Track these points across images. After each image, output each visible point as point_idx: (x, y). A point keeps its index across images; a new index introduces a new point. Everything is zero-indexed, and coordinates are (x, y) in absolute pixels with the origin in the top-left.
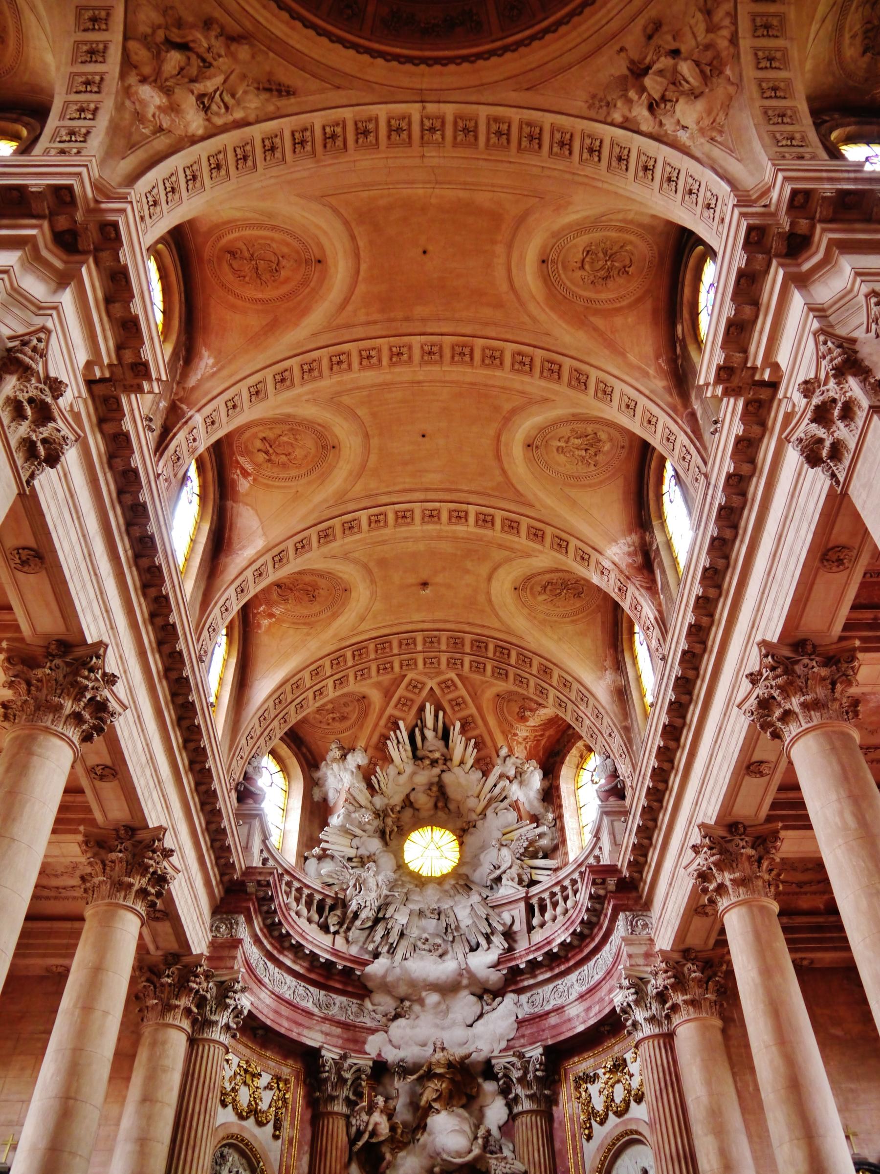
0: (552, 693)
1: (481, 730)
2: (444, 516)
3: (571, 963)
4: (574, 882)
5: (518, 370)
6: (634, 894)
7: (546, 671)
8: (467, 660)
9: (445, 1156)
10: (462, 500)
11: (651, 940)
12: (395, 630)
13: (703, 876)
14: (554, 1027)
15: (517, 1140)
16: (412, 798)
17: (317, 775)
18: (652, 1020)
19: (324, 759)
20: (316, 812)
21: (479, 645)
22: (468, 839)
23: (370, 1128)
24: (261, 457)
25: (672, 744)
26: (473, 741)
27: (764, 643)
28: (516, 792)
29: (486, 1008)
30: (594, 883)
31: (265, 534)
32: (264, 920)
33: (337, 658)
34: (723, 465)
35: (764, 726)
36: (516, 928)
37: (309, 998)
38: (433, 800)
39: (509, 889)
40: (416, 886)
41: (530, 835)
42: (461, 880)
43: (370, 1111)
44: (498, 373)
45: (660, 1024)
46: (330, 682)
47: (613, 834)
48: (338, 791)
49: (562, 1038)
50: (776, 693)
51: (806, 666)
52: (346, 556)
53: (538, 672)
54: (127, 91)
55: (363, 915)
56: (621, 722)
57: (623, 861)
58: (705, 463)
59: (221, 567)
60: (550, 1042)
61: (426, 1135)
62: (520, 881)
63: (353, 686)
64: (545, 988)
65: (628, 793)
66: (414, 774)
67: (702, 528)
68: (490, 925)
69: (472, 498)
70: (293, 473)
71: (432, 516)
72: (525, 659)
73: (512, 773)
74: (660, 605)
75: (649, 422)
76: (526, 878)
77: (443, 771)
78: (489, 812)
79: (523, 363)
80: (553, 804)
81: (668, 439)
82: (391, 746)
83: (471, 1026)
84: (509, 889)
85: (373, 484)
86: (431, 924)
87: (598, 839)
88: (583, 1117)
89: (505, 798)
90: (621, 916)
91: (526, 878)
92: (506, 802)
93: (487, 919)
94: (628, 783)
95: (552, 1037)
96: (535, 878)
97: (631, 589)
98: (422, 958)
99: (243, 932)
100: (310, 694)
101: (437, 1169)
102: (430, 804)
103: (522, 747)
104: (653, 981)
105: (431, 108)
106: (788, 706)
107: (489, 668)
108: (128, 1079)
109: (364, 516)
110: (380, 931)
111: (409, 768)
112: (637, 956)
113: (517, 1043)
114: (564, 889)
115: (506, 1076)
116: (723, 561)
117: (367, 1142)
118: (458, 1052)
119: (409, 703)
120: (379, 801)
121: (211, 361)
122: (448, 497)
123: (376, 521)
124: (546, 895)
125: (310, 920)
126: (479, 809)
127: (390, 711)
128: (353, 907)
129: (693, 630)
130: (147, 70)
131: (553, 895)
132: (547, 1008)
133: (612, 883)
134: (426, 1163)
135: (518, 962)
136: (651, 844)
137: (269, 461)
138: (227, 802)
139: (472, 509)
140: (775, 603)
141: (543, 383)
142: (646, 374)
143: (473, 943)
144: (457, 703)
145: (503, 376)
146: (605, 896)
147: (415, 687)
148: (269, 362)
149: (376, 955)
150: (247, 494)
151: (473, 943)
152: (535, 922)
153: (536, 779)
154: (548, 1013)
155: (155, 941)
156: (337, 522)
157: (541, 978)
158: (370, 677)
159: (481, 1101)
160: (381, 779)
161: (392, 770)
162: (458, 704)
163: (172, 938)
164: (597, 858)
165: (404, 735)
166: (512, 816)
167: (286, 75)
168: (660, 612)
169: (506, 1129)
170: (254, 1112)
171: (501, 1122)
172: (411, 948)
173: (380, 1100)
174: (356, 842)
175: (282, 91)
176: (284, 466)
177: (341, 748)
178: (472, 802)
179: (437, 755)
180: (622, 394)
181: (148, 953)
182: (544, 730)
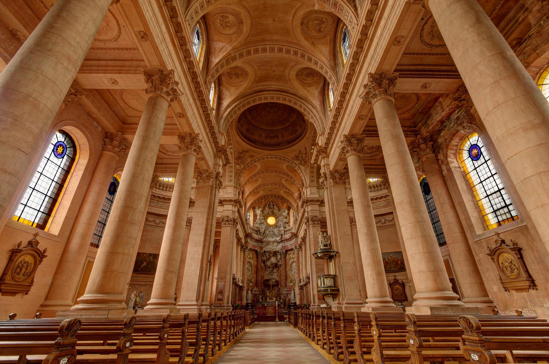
20: (255, 216)
21: (279, 197)
28: (284, 214)
33: (258, 199)
37: (256, 244)
42: (276, 226)
72: (285, 199)
79: (284, 174)
84: (282, 228)
86: (271, 233)
99: (249, 240)
118: (274, 250)
153: (287, 212)
167: (253, 154)
169: (280, 259)
170: (250, 258)
175: (252, 156)
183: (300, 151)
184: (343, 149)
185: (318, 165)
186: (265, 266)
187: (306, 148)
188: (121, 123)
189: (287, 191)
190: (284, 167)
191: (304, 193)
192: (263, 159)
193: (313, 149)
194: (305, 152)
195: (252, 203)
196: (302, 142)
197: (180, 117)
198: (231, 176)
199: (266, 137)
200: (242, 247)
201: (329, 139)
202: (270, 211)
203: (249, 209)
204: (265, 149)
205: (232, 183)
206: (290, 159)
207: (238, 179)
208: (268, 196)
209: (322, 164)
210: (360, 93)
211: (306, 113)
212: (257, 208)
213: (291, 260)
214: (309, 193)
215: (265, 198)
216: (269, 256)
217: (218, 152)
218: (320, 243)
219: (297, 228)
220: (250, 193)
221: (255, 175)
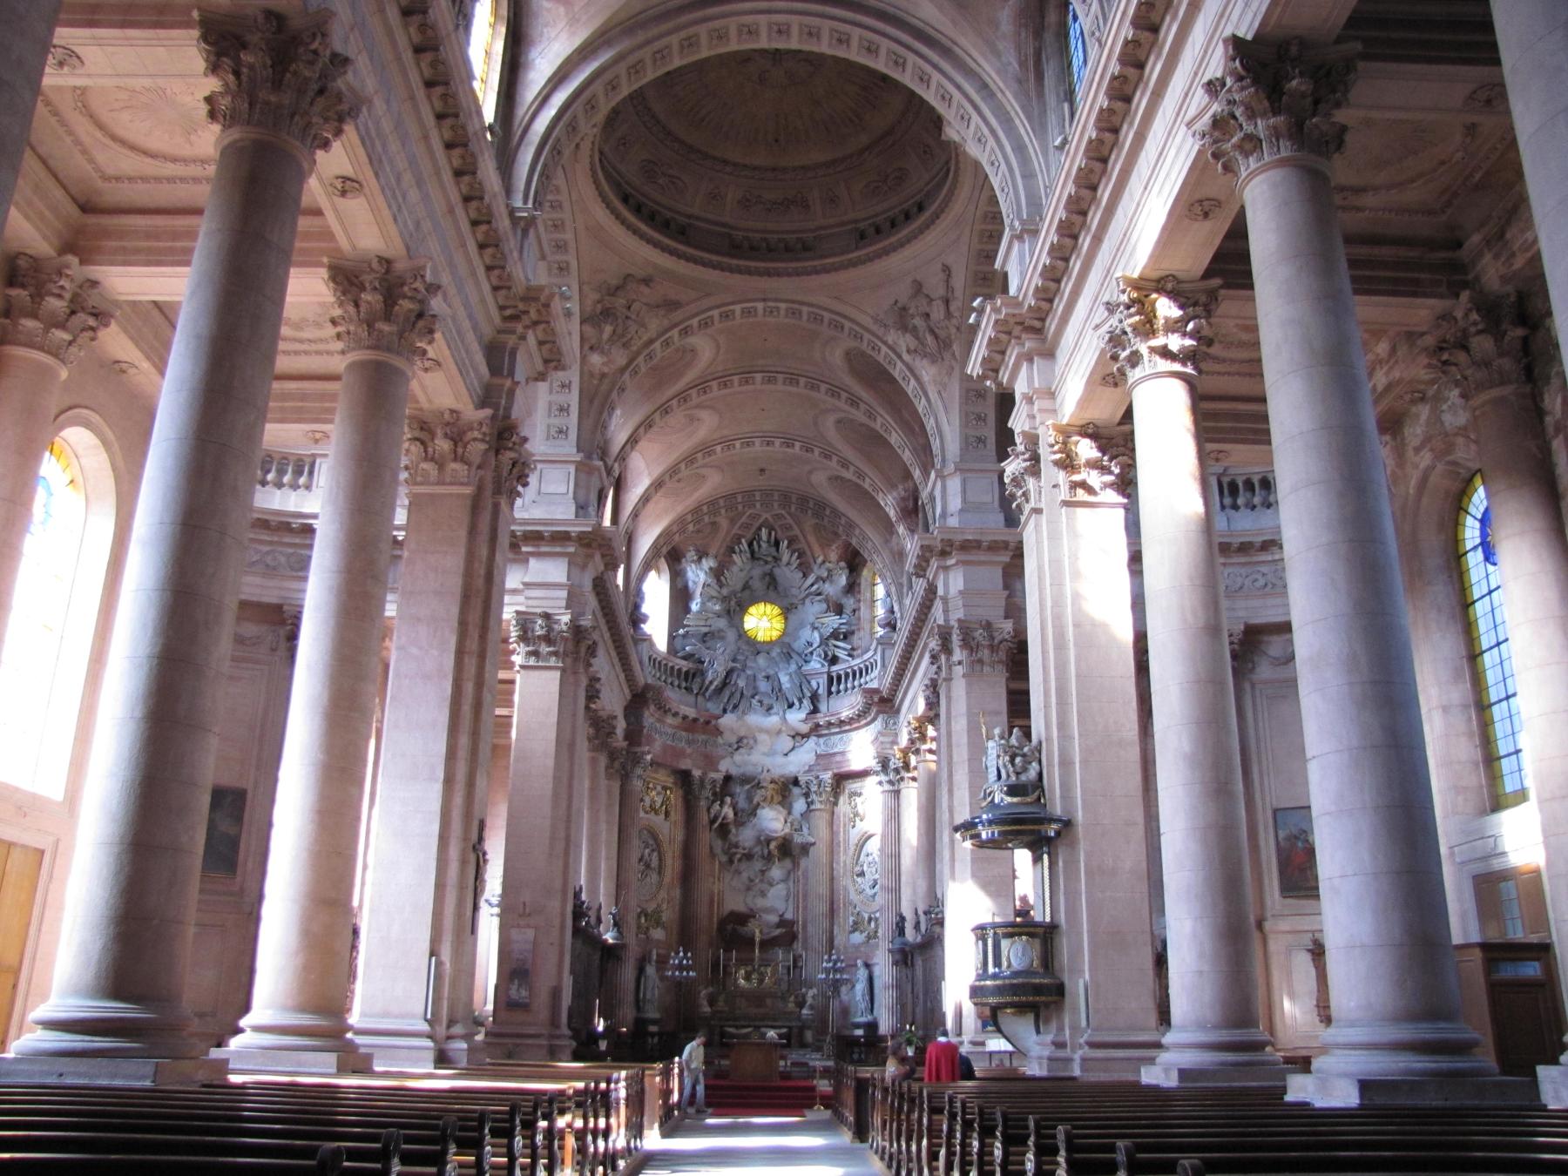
20: (680, 597)
21: (803, 500)
22: (791, 617)
33: (697, 511)
42: (785, 648)
54: (584, 358)
79: (834, 394)
84: (816, 664)
85: (726, 432)
98: (755, 711)
105: (771, 304)
110: (727, 693)
117: (722, 825)
120: (725, 591)
128: (710, 676)
130: (593, 341)
144: (789, 528)
149: (725, 711)
161: (735, 569)
166: (824, 606)
169: (806, 815)
170: (653, 809)
173: (728, 800)
175: (671, 305)
177: (697, 551)
178: (794, 591)
183: (918, 287)
184: (1117, 340)
185: (999, 384)
186: (731, 850)
187: (947, 270)
188: (73, 211)
189: (848, 475)
190: (836, 357)
191: (932, 498)
192: (726, 316)
193: (981, 312)
194: (941, 292)
195: (666, 535)
196: (930, 237)
197: (344, 193)
198: (564, 410)
199: (745, 203)
200: (613, 756)
201: (1053, 276)
203: (648, 566)
204: (739, 271)
205: (568, 448)
206: (867, 321)
207: (601, 426)
208: (749, 494)
209: (1020, 388)
210: (1192, 112)
211: (948, 114)
212: (691, 555)
214: (955, 503)
216: (750, 799)
217: (506, 319)
218: (993, 776)
219: (891, 670)
220: (657, 485)
221: (683, 397)
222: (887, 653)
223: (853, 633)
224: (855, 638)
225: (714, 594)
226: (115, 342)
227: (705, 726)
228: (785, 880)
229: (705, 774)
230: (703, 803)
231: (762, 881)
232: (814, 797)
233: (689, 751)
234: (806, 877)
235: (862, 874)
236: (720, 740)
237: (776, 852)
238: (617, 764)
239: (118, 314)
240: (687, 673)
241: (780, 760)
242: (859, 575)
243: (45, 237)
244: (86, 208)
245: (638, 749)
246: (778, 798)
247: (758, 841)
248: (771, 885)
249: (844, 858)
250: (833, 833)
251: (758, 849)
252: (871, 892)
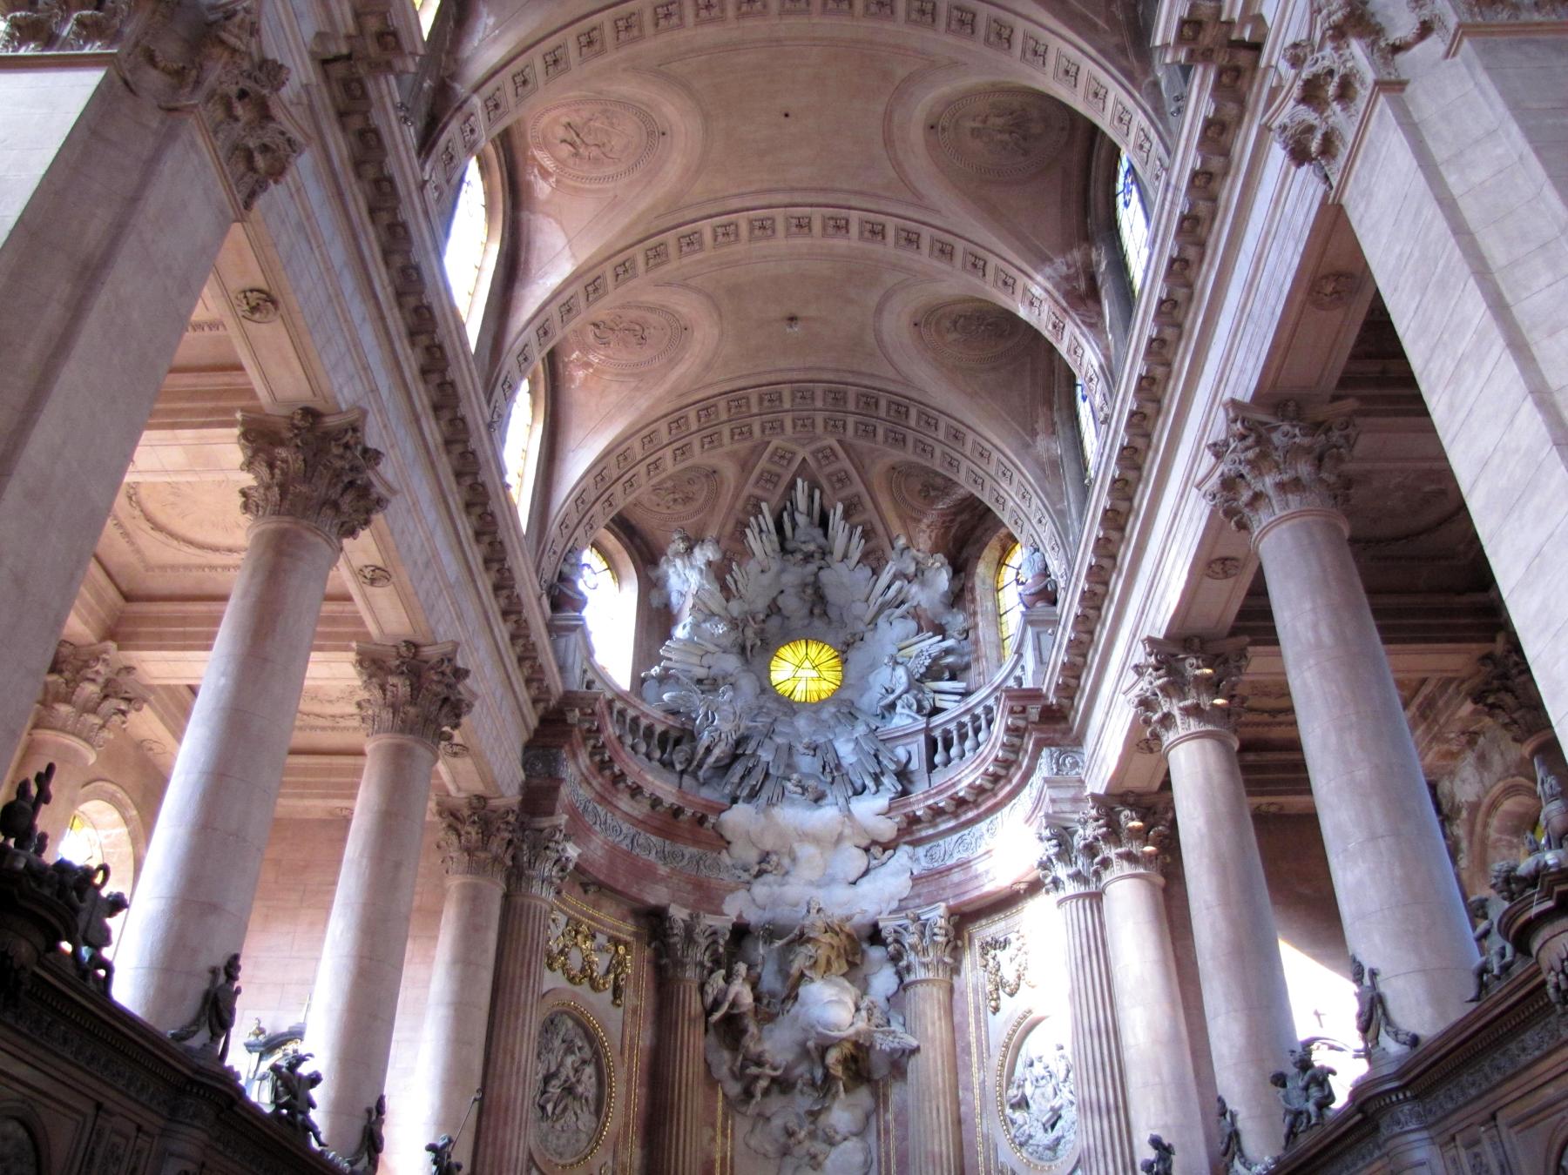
0: (965, 464)
1: (870, 514)
2: (817, 226)
3: (983, 808)
4: (988, 710)
5: (915, 22)
6: (1063, 726)
7: (957, 436)
8: (851, 420)
9: (820, 1029)
10: (841, 202)
11: (1082, 782)
12: (752, 382)
13: (1145, 704)
14: (958, 885)
15: (907, 1013)
16: (780, 602)
17: (653, 575)
18: (1077, 877)
19: (663, 553)
20: (656, 619)
21: (869, 401)
22: (853, 655)
23: (731, 997)
24: (565, 150)
25: (1114, 535)
26: (860, 529)
27: (1234, 403)
29: (874, 862)
30: (1012, 712)
31: (573, 256)
32: (591, 755)
33: (676, 420)
34: (1188, 158)
35: (1229, 513)
36: (914, 765)
37: (650, 848)
38: (809, 605)
39: (903, 719)
40: (785, 714)
41: (935, 651)
42: (844, 707)
43: (728, 979)
44: (888, 26)
45: (1086, 882)
46: (668, 453)
47: (1038, 649)
48: (682, 595)
49: (966, 897)
50: (1245, 470)
51: (1286, 434)
52: (683, 284)
53: (947, 436)
55: (717, 752)
56: (1053, 504)
57: (1049, 685)
58: (1168, 152)
59: (514, 302)
60: (952, 902)
61: (797, 1005)
62: (920, 710)
63: (698, 457)
64: (948, 839)
65: (1061, 596)
66: (782, 571)
67: (1157, 246)
68: (879, 763)
69: (853, 202)
70: (610, 170)
71: (803, 225)
73: (912, 569)
74: (1107, 348)
75: (1096, 95)
76: (927, 705)
77: (820, 568)
78: (881, 621)
80: (964, 609)
81: (1121, 120)
82: (751, 537)
83: (854, 883)
84: (903, 719)
87: (1021, 656)
88: (990, 987)
89: (903, 602)
90: (1045, 752)
91: (927, 705)
92: (904, 607)
93: (876, 756)
94: (1062, 584)
95: (955, 896)
96: (939, 704)
97: (1070, 328)
98: (793, 803)
100: (642, 469)
101: (811, 1044)
102: (805, 611)
103: (926, 536)
104: (1081, 832)
106: (1259, 487)
107: (880, 432)
108: (436, 938)
109: (706, 227)
110: (739, 769)
111: (775, 567)
112: (1062, 800)
113: (911, 903)
114: (976, 718)
115: (897, 941)
116: (1184, 290)
119: (775, 479)
120: (735, 607)
121: (491, 21)
122: (821, 199)
123: (727, 233)
124: (952, 726)
125: (648, 756)
126: (868, 618)
127: (749, 489)
128: (705, 739)
129: (1144, 383)
131: (962, 725)
132: (949, 863)
133: (1034, 712)
134: (799, 1036)
135: (915, 807)
136: (1085, 662)
137: (576, 154)
138: (536, 612)
139: (854, 216)
140: (1249, 349)
141: (950, 39)
142: (1094, 26)
143: (858, 784)
144: (842, 480)
145: (896, 30)
146: (1026, 729)
147: (782, 457)
148: (569, 19)
149: (735, 800)
150: (548, 202)
151: (858, 784)
152: (938, 759)
154: (950, 869)
155: (455, 781)
156: (670, 237)
157: (943, 827)
158: (721, 445)
159: (865, 969)
160: (738, 577)
161: (752, 567)
162: (840, 480)
163: (477, 778)
164: (1019, 680)
165: (768, 521)
166: (912, 625)
168: (1107, 357)
169: (896, 1000)
171: (890, 993)
172: (779, 790)
173: (742, 968)
174: (707, 660)
176: (596, 161)
177: (686, 539)
178: (859, 608)
179: (812, 547)
180: (1059, 54)
181: (448, 795)
182: (956, 514)
186: (747, 1069)
195: (615, 453)
202: (794, 575)
213: (1011, 1007)
215: (742, 433)
222: (1046, 640)
223: (967, 667)
224: (973, 672)
225: (715, 608)
226: (146, 723)
227: (691, 828)
228: (860, 1134)
229: (694, 917)
230: (691, 974)
231: (812, 1135)
232: (911, 957)
233: (663, 870)
234: (902, 1123)
235: (1022, 1104)
236: (725, 858)
237: (838, 1071)
238: (496, 846)
239: (152, 698)
240: (664, 736)
241: (841, 893)
242: (971, 575)
243: (86, 623)
244: (128, 597)
245: (545, 823)
246: (840, 966)
247: (805, 1053)
248: (831, 1143)
249: (981, 1076)
250: (955, 1029)
251: (802, 1069)
252: (1046, 1138)
